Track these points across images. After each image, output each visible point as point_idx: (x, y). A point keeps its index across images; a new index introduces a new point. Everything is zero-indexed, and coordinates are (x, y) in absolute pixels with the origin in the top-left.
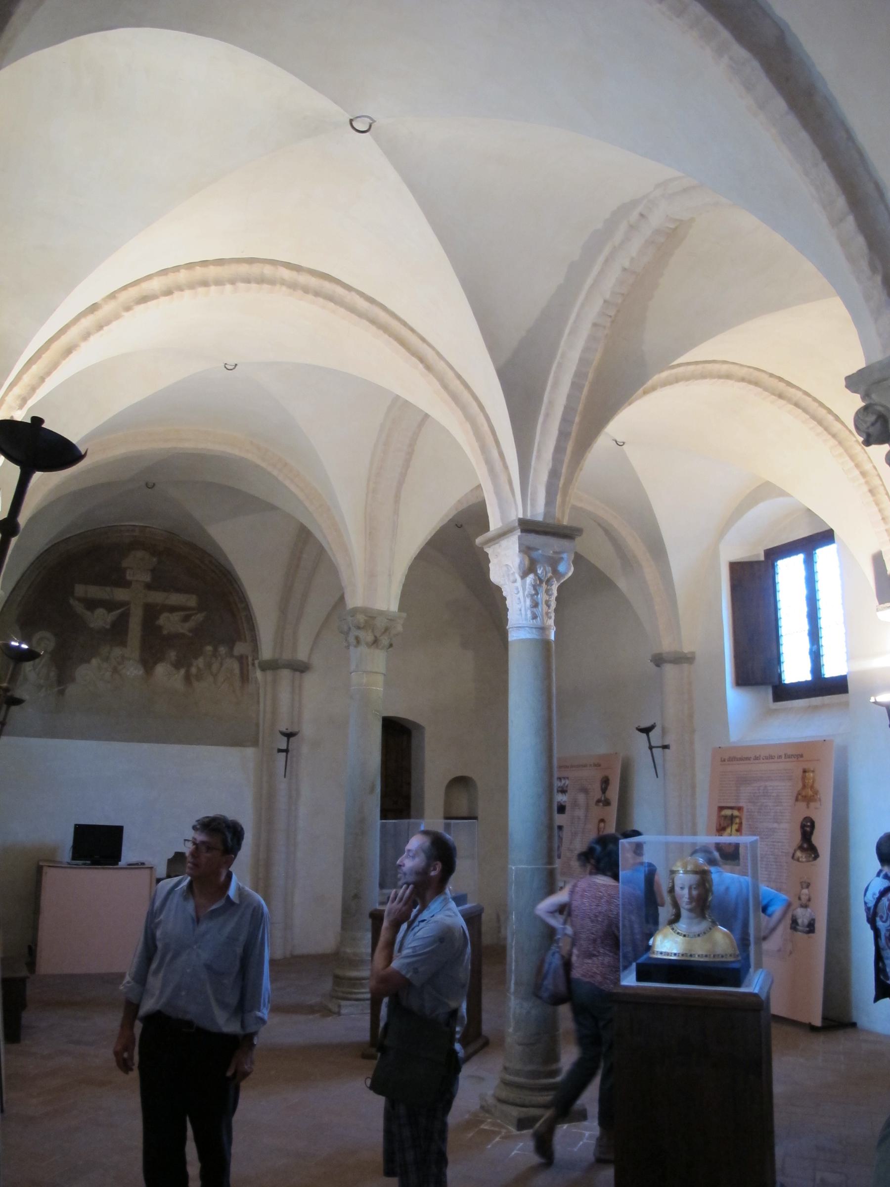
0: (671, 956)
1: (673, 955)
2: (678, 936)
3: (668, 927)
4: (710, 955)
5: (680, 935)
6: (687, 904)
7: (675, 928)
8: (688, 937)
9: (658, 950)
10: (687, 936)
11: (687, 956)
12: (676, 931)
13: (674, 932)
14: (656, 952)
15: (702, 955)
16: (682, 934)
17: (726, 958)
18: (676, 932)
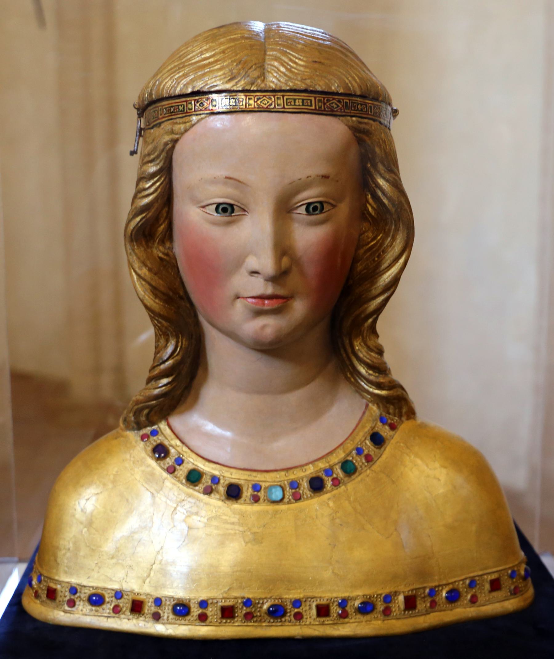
0: (157, 617)
1: (166, 612)
2: (196, 493)
3: (133, 436)
4: (388, 599)
5: (208, 491)
6: (259, 313)
7: (173, 443)
8: (256, 499)
9: (74, 580)
10: (247, 493)
11: (249, 616)
12: (180, 461)
13: (171, 471)
14: (64, 594)
15: (343, 603)
16: (215, 480)
17: (474, 600)
18: (182, 471)
